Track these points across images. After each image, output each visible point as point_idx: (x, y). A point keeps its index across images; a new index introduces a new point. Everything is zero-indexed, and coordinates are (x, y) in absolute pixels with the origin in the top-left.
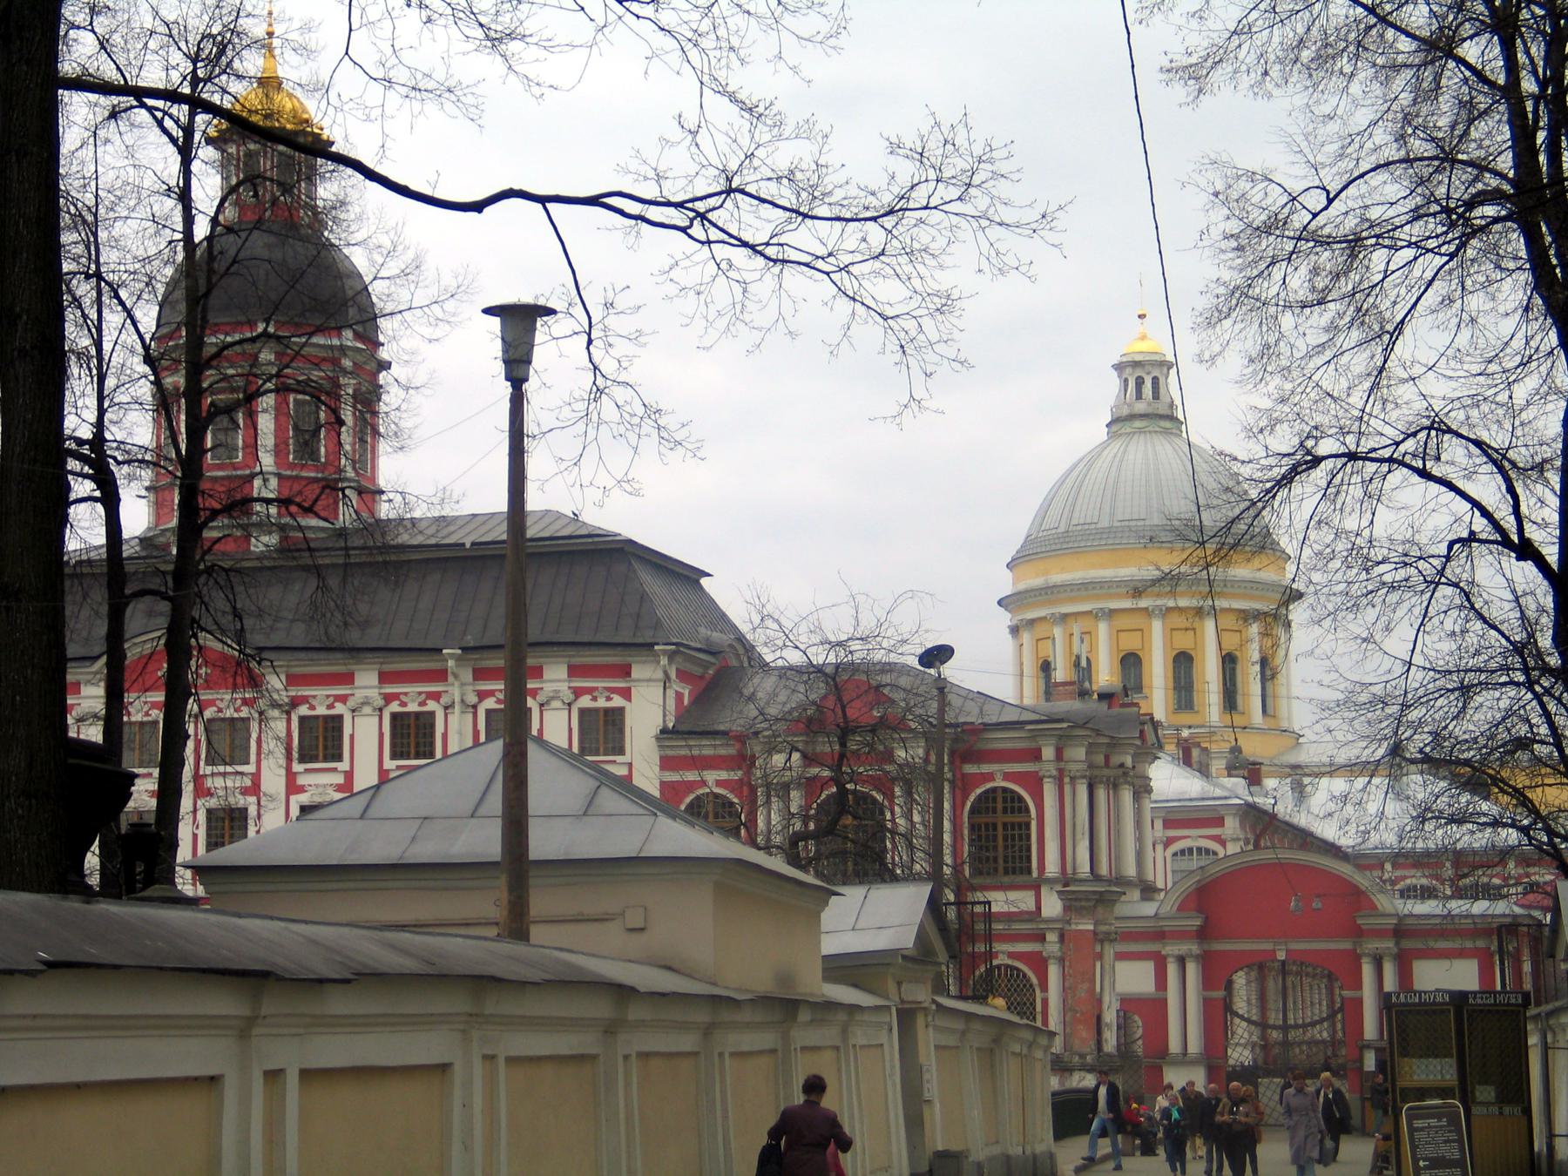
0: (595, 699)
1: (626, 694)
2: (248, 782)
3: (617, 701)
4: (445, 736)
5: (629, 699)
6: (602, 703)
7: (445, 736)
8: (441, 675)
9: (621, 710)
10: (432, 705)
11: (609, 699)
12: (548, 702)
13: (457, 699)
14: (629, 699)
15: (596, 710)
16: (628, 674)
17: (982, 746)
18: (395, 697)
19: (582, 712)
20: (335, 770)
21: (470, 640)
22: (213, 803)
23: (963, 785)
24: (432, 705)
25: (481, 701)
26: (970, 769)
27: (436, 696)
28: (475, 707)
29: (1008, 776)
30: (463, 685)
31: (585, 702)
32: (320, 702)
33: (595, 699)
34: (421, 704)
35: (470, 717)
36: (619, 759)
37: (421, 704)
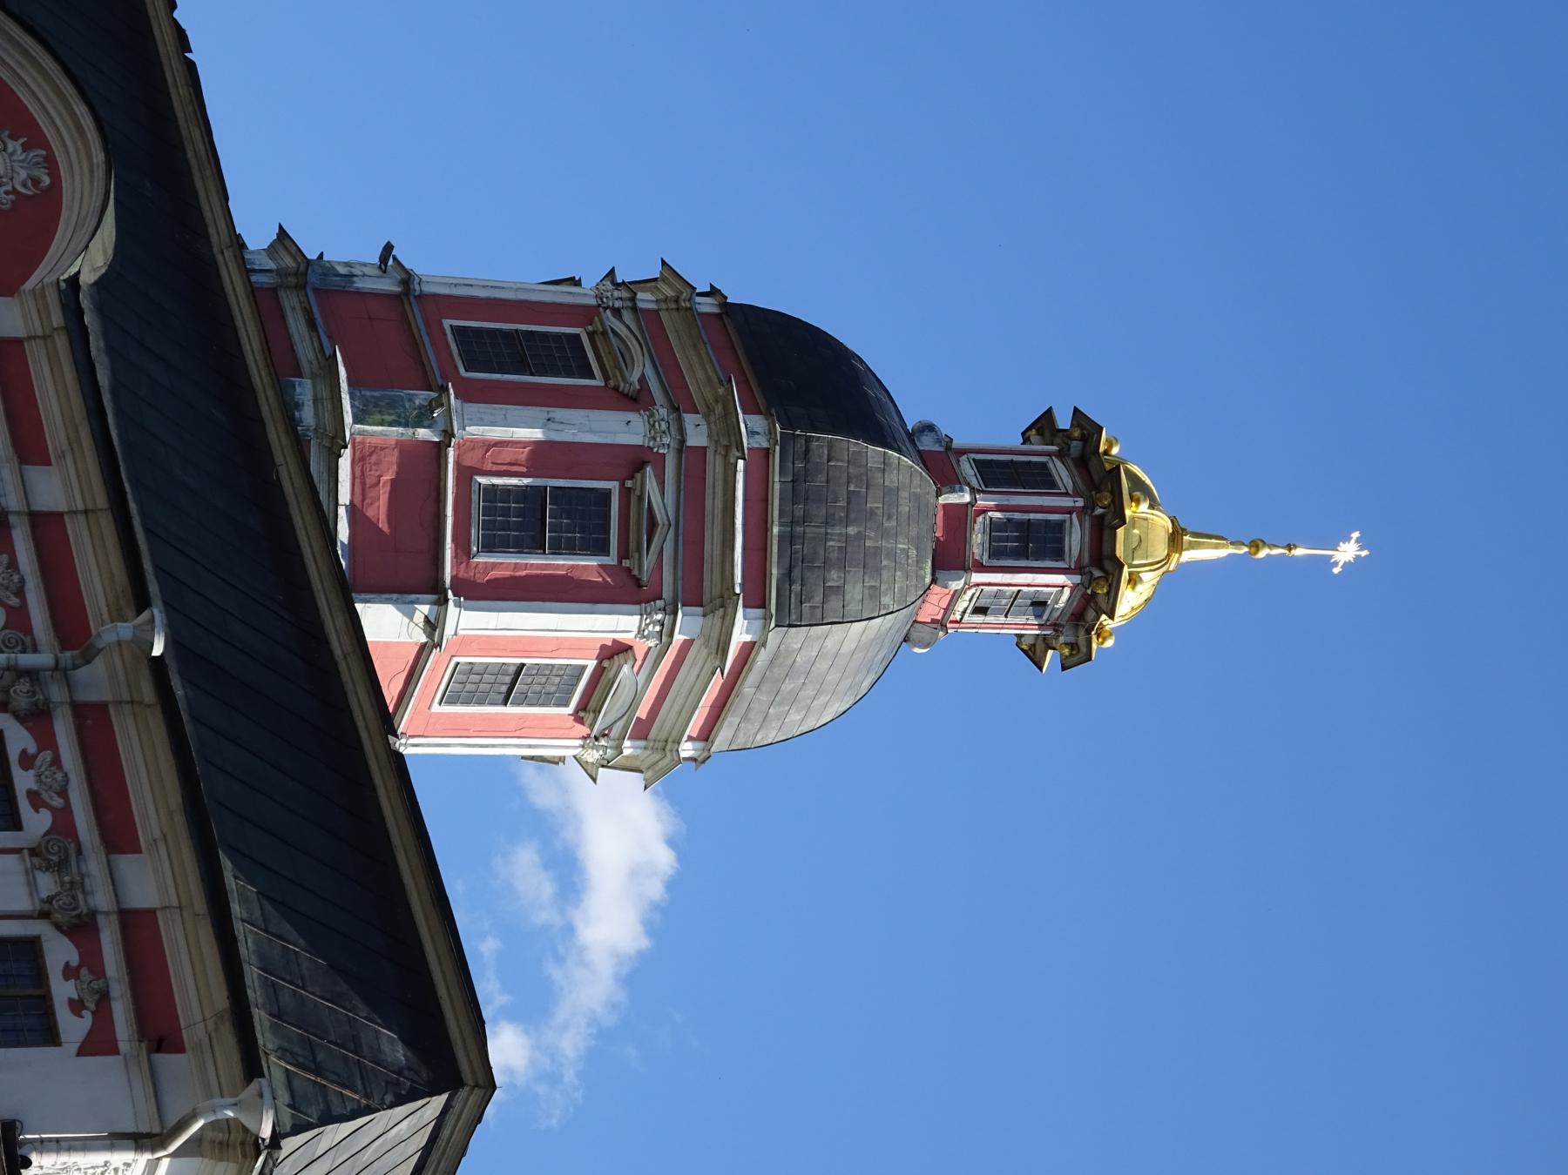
0: (69, 972)
1: (99, 1043)
3: (73, 1027)
5: (83, 1051)
6: (62, 991)
8: (72, 629)
9: (49, 1035)
11: (76, 1006)
12: (48, 867)
13: (27, 660)
14: (83, 1051)
15: (40, 975)
16: (159, 1050)
19: (31, 948)
25: (21, 718)
31: (59, 952)
33: (69, 972)
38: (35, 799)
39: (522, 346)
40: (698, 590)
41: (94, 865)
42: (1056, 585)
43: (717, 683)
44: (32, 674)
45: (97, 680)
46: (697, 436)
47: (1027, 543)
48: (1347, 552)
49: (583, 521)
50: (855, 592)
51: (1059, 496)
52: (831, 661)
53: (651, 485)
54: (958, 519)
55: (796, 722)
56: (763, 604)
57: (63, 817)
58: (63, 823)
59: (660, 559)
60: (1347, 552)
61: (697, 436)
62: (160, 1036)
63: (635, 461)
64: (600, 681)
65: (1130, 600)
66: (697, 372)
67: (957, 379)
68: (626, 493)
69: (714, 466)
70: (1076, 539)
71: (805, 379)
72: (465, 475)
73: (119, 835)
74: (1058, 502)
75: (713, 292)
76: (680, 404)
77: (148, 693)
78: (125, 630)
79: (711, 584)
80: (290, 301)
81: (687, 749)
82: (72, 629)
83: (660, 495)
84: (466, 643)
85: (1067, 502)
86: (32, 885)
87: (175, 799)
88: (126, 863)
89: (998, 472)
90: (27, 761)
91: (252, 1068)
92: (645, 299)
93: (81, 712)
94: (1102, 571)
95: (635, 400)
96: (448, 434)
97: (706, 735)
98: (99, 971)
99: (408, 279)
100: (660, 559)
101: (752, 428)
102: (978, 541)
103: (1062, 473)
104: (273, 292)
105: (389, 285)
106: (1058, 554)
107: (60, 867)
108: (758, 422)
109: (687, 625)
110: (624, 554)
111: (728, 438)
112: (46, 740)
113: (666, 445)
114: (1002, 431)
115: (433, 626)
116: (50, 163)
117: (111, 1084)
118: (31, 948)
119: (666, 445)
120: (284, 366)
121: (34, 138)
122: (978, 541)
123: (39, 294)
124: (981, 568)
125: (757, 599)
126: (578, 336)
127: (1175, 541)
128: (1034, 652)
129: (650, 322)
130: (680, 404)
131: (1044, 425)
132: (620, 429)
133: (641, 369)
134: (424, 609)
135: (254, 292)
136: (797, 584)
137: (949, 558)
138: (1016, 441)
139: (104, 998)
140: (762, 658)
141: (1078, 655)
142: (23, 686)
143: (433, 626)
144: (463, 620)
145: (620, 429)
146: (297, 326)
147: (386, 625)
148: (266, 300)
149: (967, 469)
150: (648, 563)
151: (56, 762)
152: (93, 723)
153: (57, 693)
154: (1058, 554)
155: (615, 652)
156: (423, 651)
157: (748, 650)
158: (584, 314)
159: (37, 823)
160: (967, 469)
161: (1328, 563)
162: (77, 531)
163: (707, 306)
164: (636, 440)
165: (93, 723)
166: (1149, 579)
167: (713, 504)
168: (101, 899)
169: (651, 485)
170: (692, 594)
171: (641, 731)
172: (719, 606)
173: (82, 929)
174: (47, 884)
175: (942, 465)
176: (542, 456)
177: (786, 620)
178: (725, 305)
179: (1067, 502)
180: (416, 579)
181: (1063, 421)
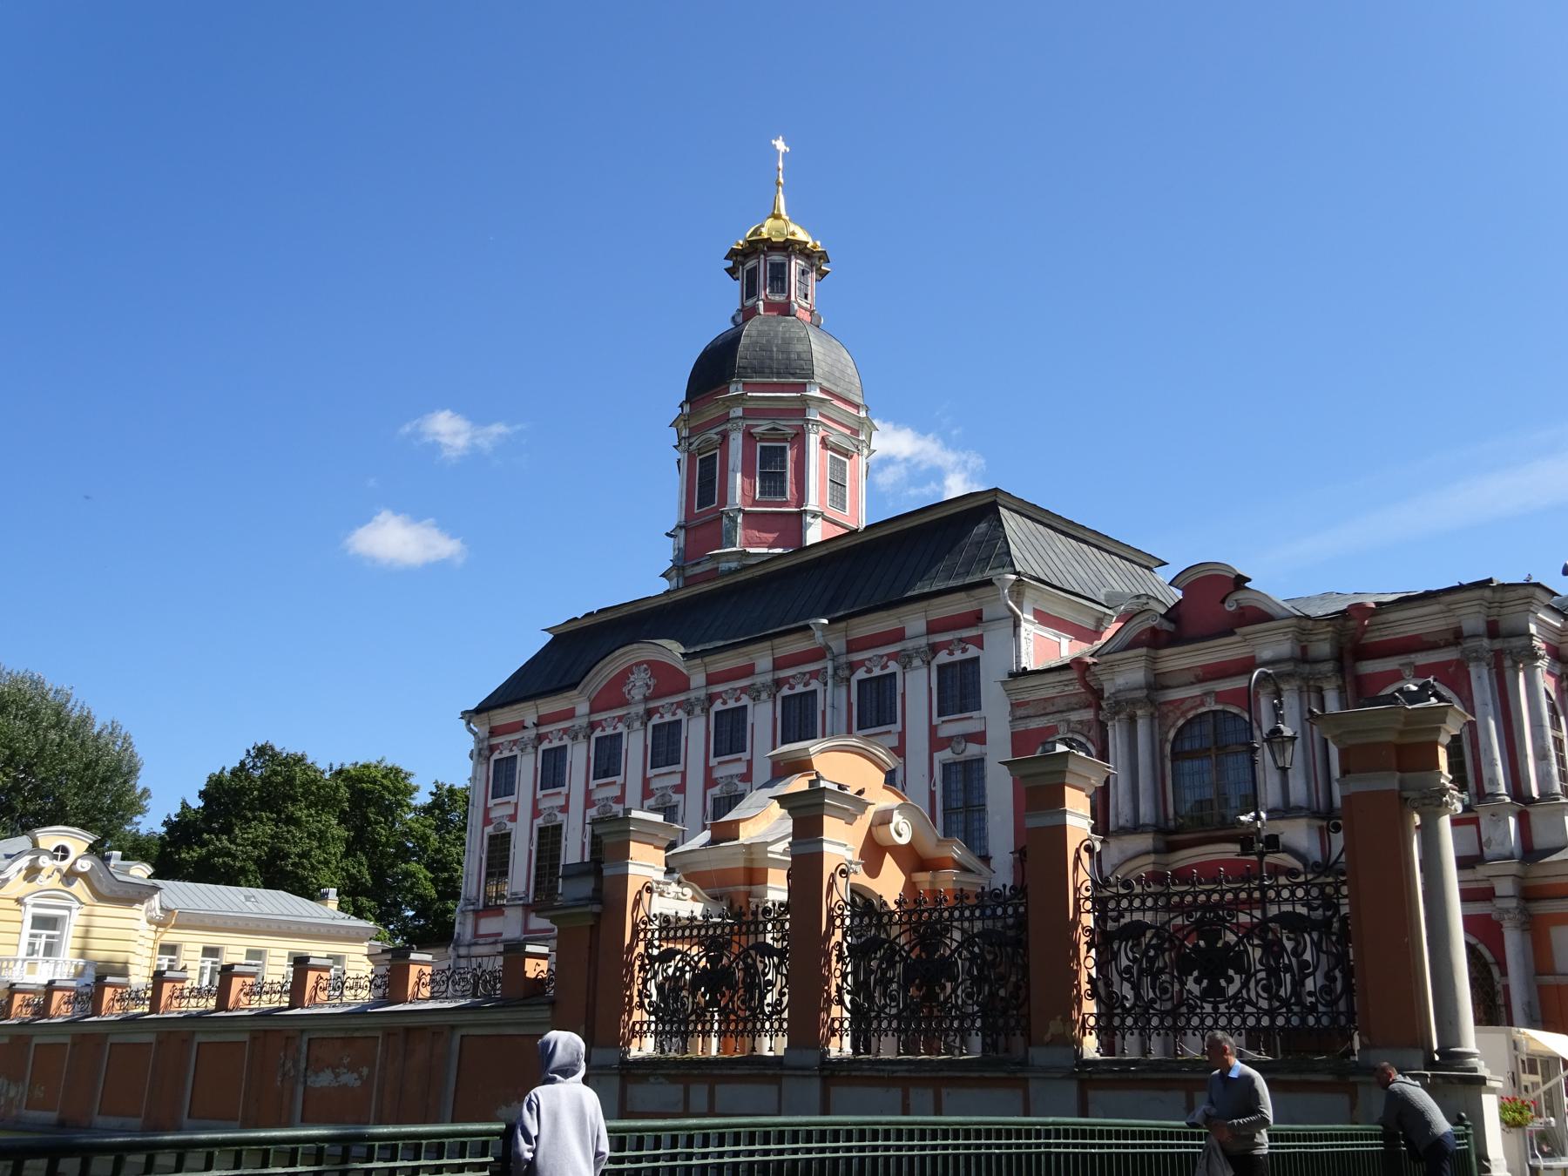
1: (979, 642)
2: (744, 770)
3: (972, 651)
4: (824, 713)
6: (958, 656)
8: (818, 654)
9: (976, 660)
10: (815, 685)
11: (964, 650)
13: (830, 671)
17: (1374, 637)
19: (941, 668)
26: (1370, 667)
28: (848, 680)
31: (943, 657)
33: (951, 654)
34: (806, 685)
35: (844, 691)
36: (974, 714)
37: (806, 685)
38: (884, 667)
39: (704, 482)
40: (799, 411)
41: (909, 644)
42: (796, 265)
43: (835, 402)
44: (836, 669)
45: (838, 645)
46: (739, 412)
47: (779, 277)
48: (780, 145)
49: (773, 457)
50: (799, 347)
51: (760, 264)
52: (828, 358)
54: (770, 306)
55: (851, 370)
56: (804, 385)
57: (891, 657)
59: (787, 426)
60: (780, 145)
62: (976, 618)
63: (749, 436)
65: (801, 235)
66: (713, 412)
67: (714, 308)
68: (762, 440)
70: (777, 258)
71: (715, 369)
72: (755, 503)
73: (898, 635)
74: (762, 265)
75: (681, 406)
76: (726, 419)
77: (842, 625)
78: (818, 634)
79: (797, 405)
80: (689, 572)
81: (863, 414)
82: (818, 654)
83: (762, 426)
84: (822, 502)
86: (917, 668)
87: (884, 614)
88: (908, 633)
89: (751, 290)
90: (869, 671)
91: (988, 583)
92: (685, 433)
93: (850, 650)
94: (789, 247)
95: (725, 437)
96: (740, 510)
97: (857, 407)
98: (950, 642)
99: (679, 527)
100: (787, 426)
101: (735, 390)
102: (778, 298)
103: (750, 264)
104: (686, 579)
105: (682, 534)
106: (783, 265)
107: (910, 657)
108: (732, 387)
109: (813, 415)
110: (785, 440)
111: (739, 399)
112: (861, 663)
113: (742, 424)
114: (735, 288)
115: (815, 516)
116: (638, 664)
117: (994, 637)
118: (941, 668)
119: (742, 424)
120: (714, 574)
122: (778, 298)
123: (689, 668)
124: (789, 296)
125: (803, 387)
127: (777, 217)
128: (823, 274)
129: (694, 431)
130: (726, 419)
131: (731, 272)
132: (736, 442)
133: (713, 435)
134: (809, 519)
135: (686, 586)
136: (797, 371)
137: (785, 310)
138: (738, 283)
139: (961, 640)
140: (826, 384)
141: (824, 256)
142: (840, 673)
144: (812, 504)
145: (736, 442)
147: (815, 533)
148: (689, 582)
149: (749, 303)
150: (789, 431)
151: (869, 659)
152: (853, 646)
153: (843, 660)
154: (783, 265)
155: (824, 443)
157: (823, 390)
158: (691, 457)
159: (893, 667)
160: (749, 303)
161: (785, 154)
162: (780, 653)
163: (687, 408)
165: (853, 646)
166: (792, 227)
167: (765, 405)
168: (923, 641)
170: (801, 413)
171: (856, 432)
172: (806, 401)
173: (934, 649)
174: (917, 662)
175: (748, 313)
176: (748, 473)
178: (687, 401)
180: (797, 521)
181: (730, 264)
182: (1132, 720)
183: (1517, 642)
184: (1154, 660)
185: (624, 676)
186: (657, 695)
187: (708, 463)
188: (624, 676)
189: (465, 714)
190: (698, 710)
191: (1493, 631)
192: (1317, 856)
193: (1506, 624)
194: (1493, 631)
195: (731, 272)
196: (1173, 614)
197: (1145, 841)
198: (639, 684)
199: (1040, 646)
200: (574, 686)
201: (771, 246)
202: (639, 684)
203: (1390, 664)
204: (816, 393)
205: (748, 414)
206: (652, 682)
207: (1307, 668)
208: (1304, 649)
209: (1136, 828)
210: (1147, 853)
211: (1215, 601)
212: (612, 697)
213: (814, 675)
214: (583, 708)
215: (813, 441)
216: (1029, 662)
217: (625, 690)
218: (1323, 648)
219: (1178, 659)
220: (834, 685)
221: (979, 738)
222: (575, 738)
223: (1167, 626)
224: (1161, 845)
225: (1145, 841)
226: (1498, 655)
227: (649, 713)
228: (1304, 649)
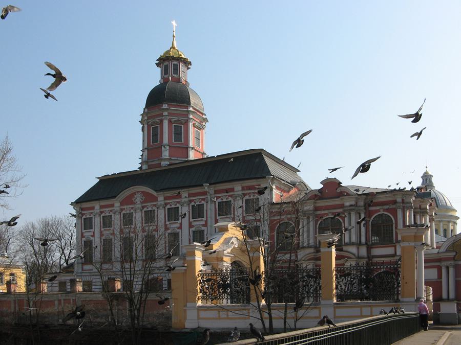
4: (207, 211)
7: (207, 211)
8: (205, 193)
10: (203, 202)
12: (236, 198)
13: (209, 199)
17: (375, 201)
18: (193, 200)
20: (177, 223)
21: (213, 182)
22: (169, 231)
23: (369, 214)
24: (203, 202)
26: (372, 208)
27: (203, 199)
29: (385, 210)
30: (211, 195)
31: (247, 197)
32: (173, 203)
35: (213, 205)
41: (236, 193)
43: (198, 113)
47: (176, 70)
48: (174, 23)
53: (173, 120)
56: (188, 106)
58: (231, 196)
60: (174, 23)
61: (166, 113)
63: (170, 122)
64: (197, 127)
69: (170, 111)
70: (175, 62)
71: (156, 98)
74: (171, 65)
75: (144, 109)
78: (206, 188)
80: (150, 164)
82: (205, 193)
83: (175, 119)
84: (193, 145)
85: (170, 63)
92: (146, 118)
93: (215, 193)
95: (162, 121)
101: (165, 106)
102: (176, 76)
103: (166, 63)
104: (149, 166)
105: (146, 151)
107: (236, 197)
108: (164, 105)
111: (166, 109)
114: (158, 71)
115: (193, 148)
116: (138, 192)
121: (135, 193)
123: (158, 195)
124: (180, 76)
125: (187, 107)
126: (153, 128)
129: (149, 118)
131: (158, 65)
132: (166, 123)
133: (157, 120)
134: (190, 149)
137: (178, 80)
138: (159, 68)
143: (193, 148)
144: (191, 145)
145: (166, 123)
146: (153, 163)
149: (166, 77)
151: (222, 196)
155: (194, 125)
156: (195, 150)
157: (194, 108)
158: (149, 127)
162: (190, 192)
163: (146, 110)
164: (167, 122)
167: (175, 112)
168: (240, 193)
169: (173, 120)
172: (189, 112)
173: (244, 195)
177: (189, 103)
179: (170, 63)
181: (158, 62)
182: (308, 218)
183: (408, 205)
184: (315, 203)
185: (132, 195)
186: (145, 202)
187: (155, 129)
188: (132, 195)
189: (72, 204)
190: (161, 208)
191: (403, 202)
192: (357, 255)
193: (406, 200)
194: (403, 202)
195: (158, 65)
196: (320, 191)
197: (312, 250)
198: (138, 199)
199: (276, 195)
200: (115, 197)
201: (173, 58)
202: (138, 199)
203: (378, 208)
204: (191, 109)
205: (169, 114)
206: (144, 198)
207: (357, 208)
208: (357, 203)
209: (309, 247)
210: (312, 253)
211: (332, 187)
212: (129, 200)
213: (203, 199)
214: (117, 204)
215: (191, 124)
216: (274, 201)
217: (133, 199)
218: (361, 203)
219: (321, 203)
220: (211, 203)
221: (260, 221)
222: (114, 213)
223: (319, 194)
224: (315, 251)
225: (312, 250)
226: (404, 207)
227: (143, 207)
228: (357, 203)
